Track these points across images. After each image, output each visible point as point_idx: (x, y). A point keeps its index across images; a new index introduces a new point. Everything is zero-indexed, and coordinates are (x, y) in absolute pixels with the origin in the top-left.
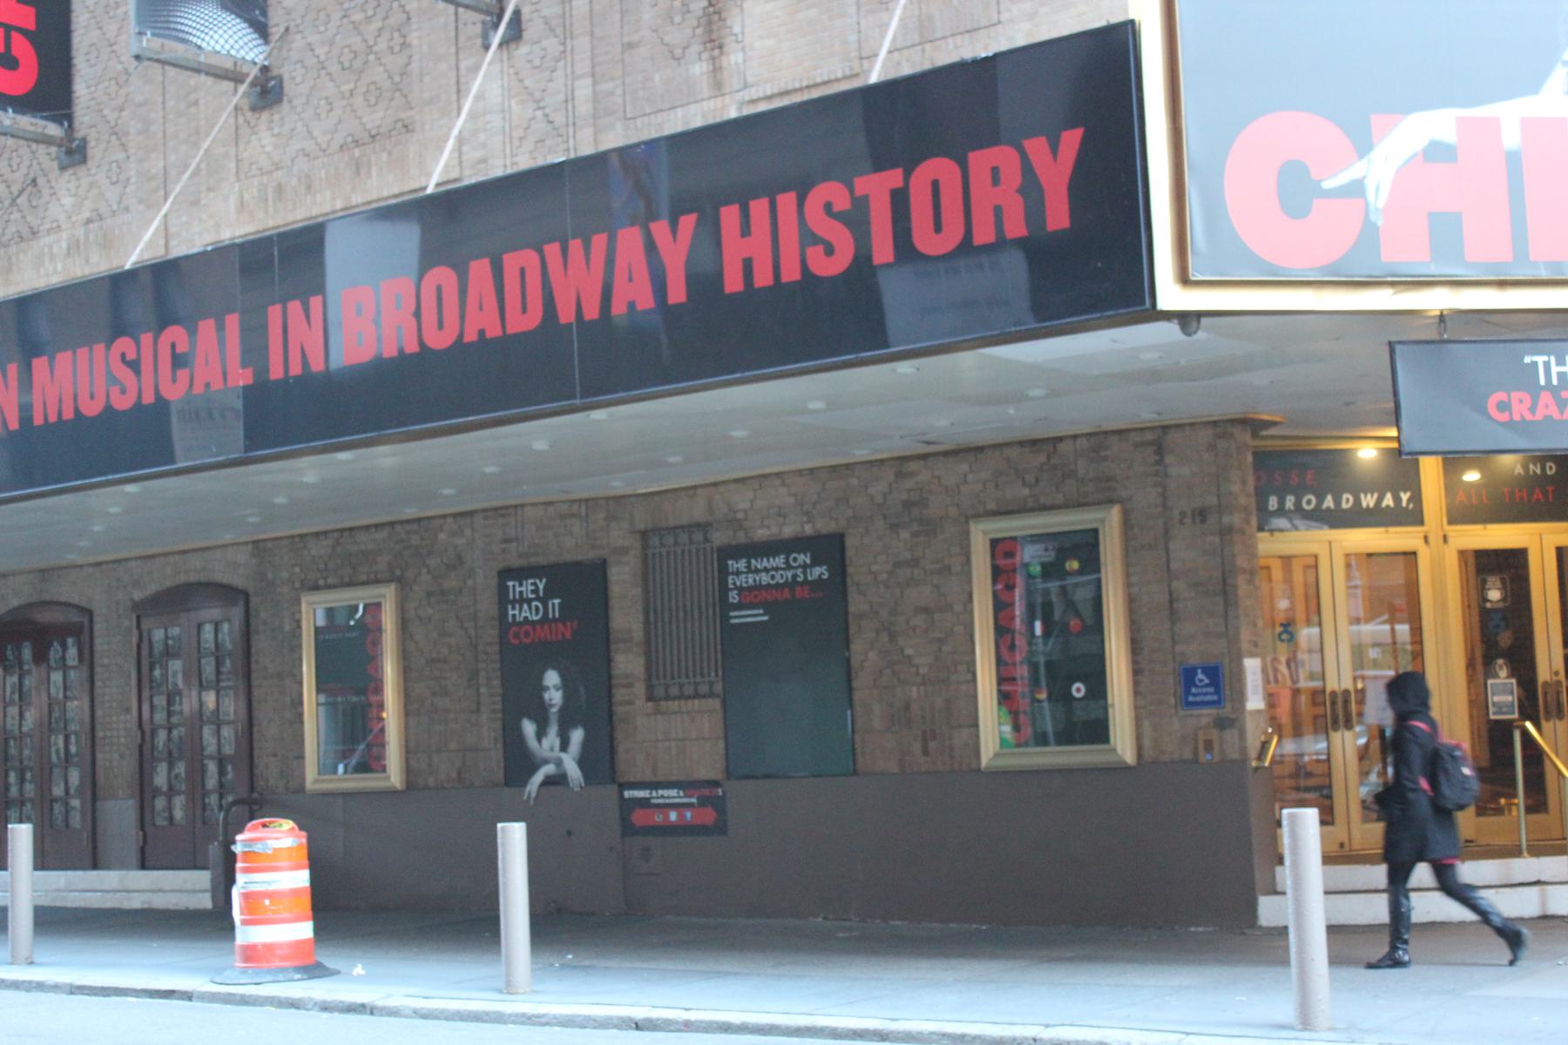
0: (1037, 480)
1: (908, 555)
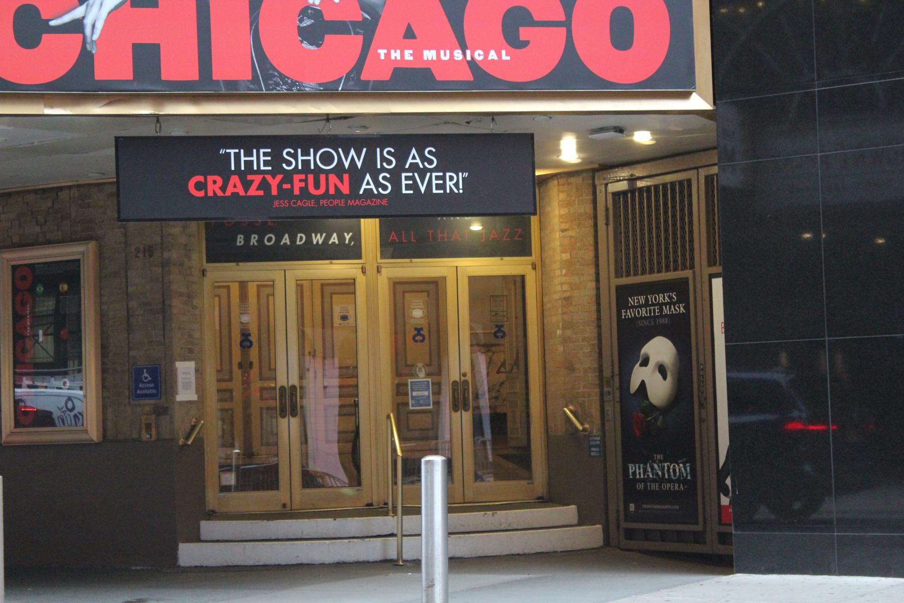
0: (46, 221)
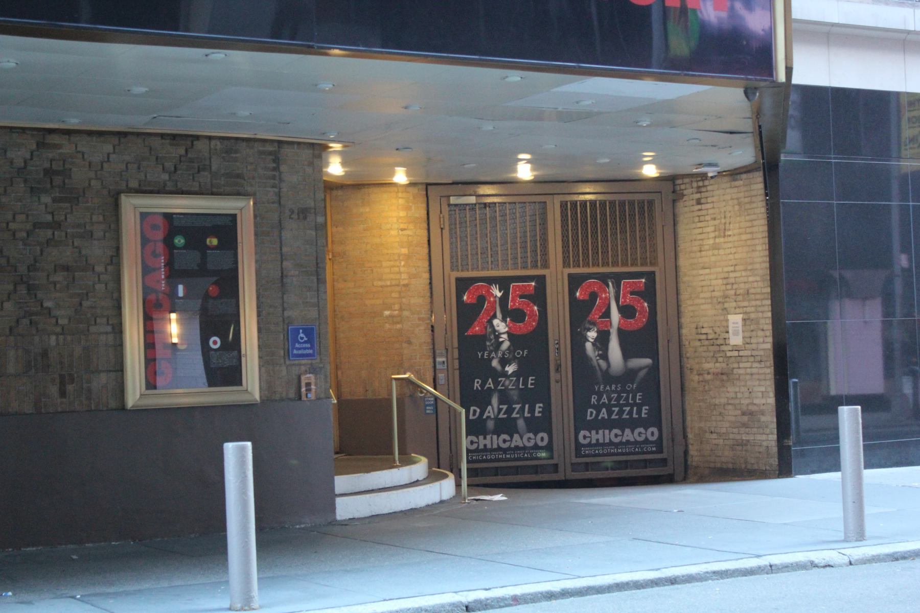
1: (49, 218)
